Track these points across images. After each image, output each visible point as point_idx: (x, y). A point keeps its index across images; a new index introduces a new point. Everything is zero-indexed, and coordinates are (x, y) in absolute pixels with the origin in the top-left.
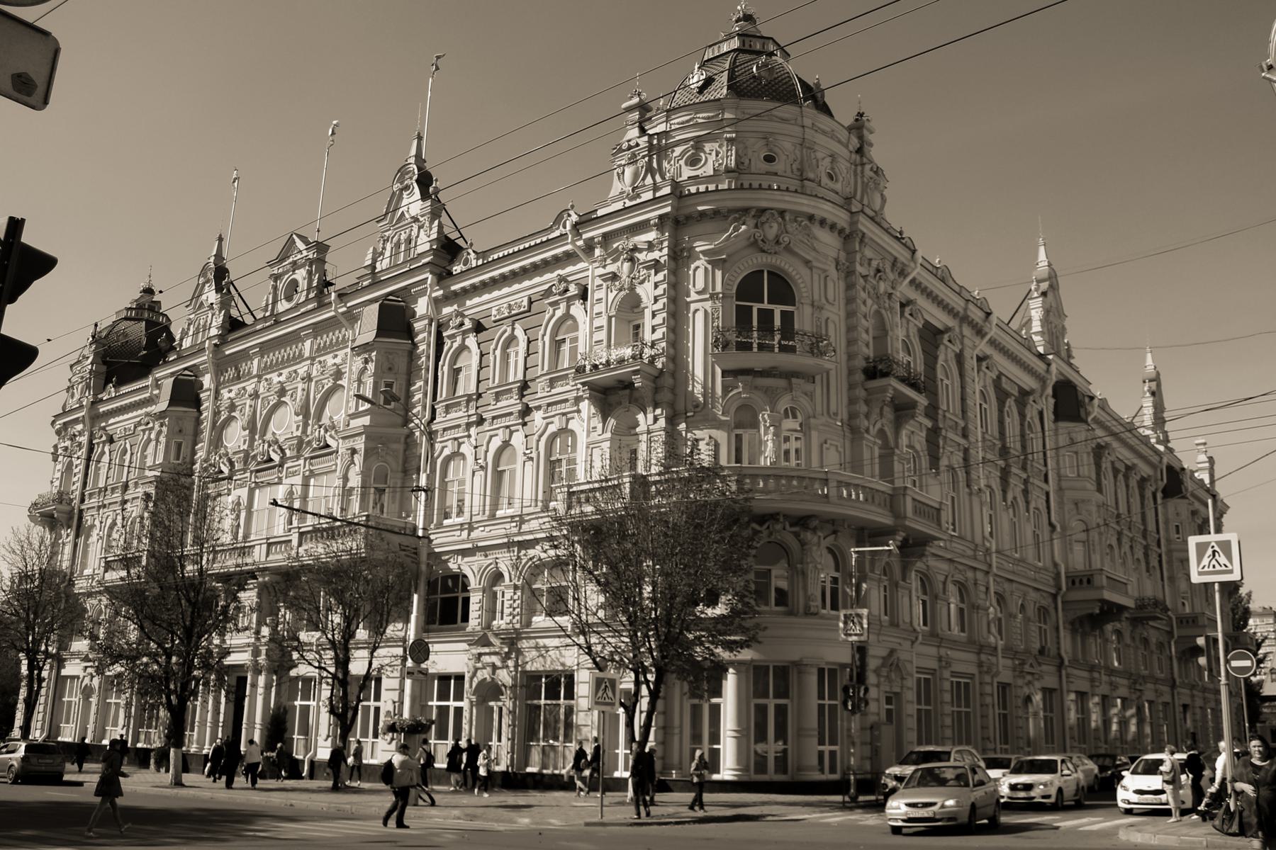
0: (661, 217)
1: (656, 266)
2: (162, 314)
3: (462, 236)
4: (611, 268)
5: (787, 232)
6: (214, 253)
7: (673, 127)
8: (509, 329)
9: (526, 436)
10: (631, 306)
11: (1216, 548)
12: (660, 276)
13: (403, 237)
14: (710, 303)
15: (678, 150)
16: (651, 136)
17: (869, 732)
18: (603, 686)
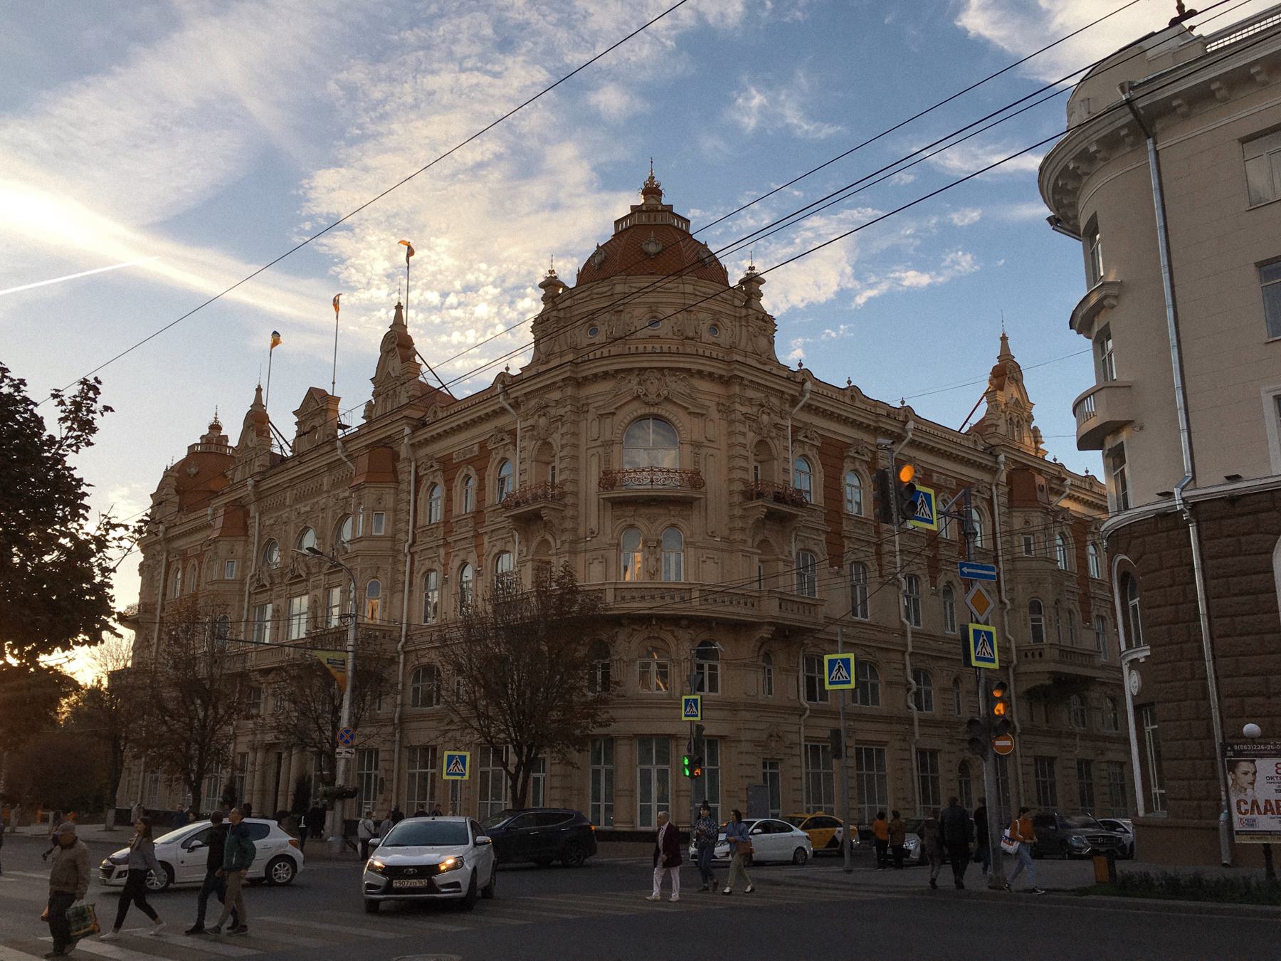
0: (563, 380)
8: (465, 470)
17: (745, 791)
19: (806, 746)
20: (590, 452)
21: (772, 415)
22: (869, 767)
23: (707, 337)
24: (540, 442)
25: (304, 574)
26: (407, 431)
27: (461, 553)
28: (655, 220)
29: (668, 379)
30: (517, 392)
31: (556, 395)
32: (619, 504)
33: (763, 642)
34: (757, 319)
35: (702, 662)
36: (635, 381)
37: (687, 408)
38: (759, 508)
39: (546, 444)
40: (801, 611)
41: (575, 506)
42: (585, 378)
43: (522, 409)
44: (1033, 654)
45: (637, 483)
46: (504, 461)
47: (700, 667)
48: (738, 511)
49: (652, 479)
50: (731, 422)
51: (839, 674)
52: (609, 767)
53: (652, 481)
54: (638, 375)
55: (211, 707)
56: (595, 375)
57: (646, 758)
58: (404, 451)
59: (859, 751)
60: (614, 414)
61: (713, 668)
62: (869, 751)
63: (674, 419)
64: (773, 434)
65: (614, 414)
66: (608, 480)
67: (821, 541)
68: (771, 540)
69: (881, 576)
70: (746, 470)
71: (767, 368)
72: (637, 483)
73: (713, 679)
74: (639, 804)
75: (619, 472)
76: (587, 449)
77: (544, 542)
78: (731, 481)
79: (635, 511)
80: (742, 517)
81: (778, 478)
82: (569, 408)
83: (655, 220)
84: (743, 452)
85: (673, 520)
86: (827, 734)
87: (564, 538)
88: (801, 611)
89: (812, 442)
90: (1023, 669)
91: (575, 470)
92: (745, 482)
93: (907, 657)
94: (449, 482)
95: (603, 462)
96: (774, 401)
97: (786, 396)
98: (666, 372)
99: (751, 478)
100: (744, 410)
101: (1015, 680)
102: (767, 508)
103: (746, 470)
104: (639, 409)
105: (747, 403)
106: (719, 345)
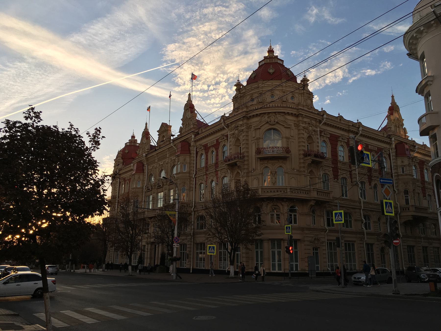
3: (204, 121)
5: (277, 118)
8: (212, 149)
9: (217, 178)
11: (339, 214)
18: (211, 248)
19: (327, 242)
21: (313, 127)
22: (350, 250)
23: (290, 101)
24: (236, 139)
25: (162, 185)
26: (193, 136)
27: (211, 177)
28: (272, 61)
29: (278, 116)
30: (228, 122)
31: (241, 123)
32: (262, 159)
33: (312, 206)
34: (307, 94)
35: (291, 213)
36: (266, 117)
37: (284, 126)
38: (309, 160)
39: (238, 140)
40: (324, 195)
41: (248, 160)
42: (250, 117)
43: (230, 128)
44: (406, 209)
45: (268, 152)
46: (224, 145)
47: (291, 215)
48: (302, 161)
49: (273, 150)
50: (299, 130)
51: (338, 218)
52: (261, 250)
53: (273, 151)
54: (268, 115)
55: (134, 230)
56: (253, 115)
57: (273, 247)
58: (192, 144)
59: (345, 244)
60: (260, 128)
61: (295, 216)
62: (349, 244)
63: (280, 130)
64: (313, 134)
65: (260, 128)
66: (259, 151)
67: (331, 170)
68: (314, 171)
69: (352, 182)
70: (305, 146)
71: (311, 111)
72: (268, 152)
73: (295, 219)
74: (271, 263)
75: (262, 148)
76: (251, 141)
77: (238, 173)
78: (299, 150)
79: (268, 162)
80: (303, 163)
81: (315, 149)
82: (245, 127)
83: (272, 61)
84: (303, 140)
85: (281, 164)
86: (335, 238)
87: (244, 172)
88: (324, 195)
89: (326, 136)
90: (403, 214)
91: (247, 148)
92: (304, 151)
93: (362, 211)
94: (207, 153)
95: (256, 146)
96: (313, 122)
97: (318, 120)
98: (277, 113)
99: (306, 149)
100: (303, 125)
101: (400, 218)
102: (312, 159)
103: (305, 146)
105: (304, 123)
106: (294, 103)
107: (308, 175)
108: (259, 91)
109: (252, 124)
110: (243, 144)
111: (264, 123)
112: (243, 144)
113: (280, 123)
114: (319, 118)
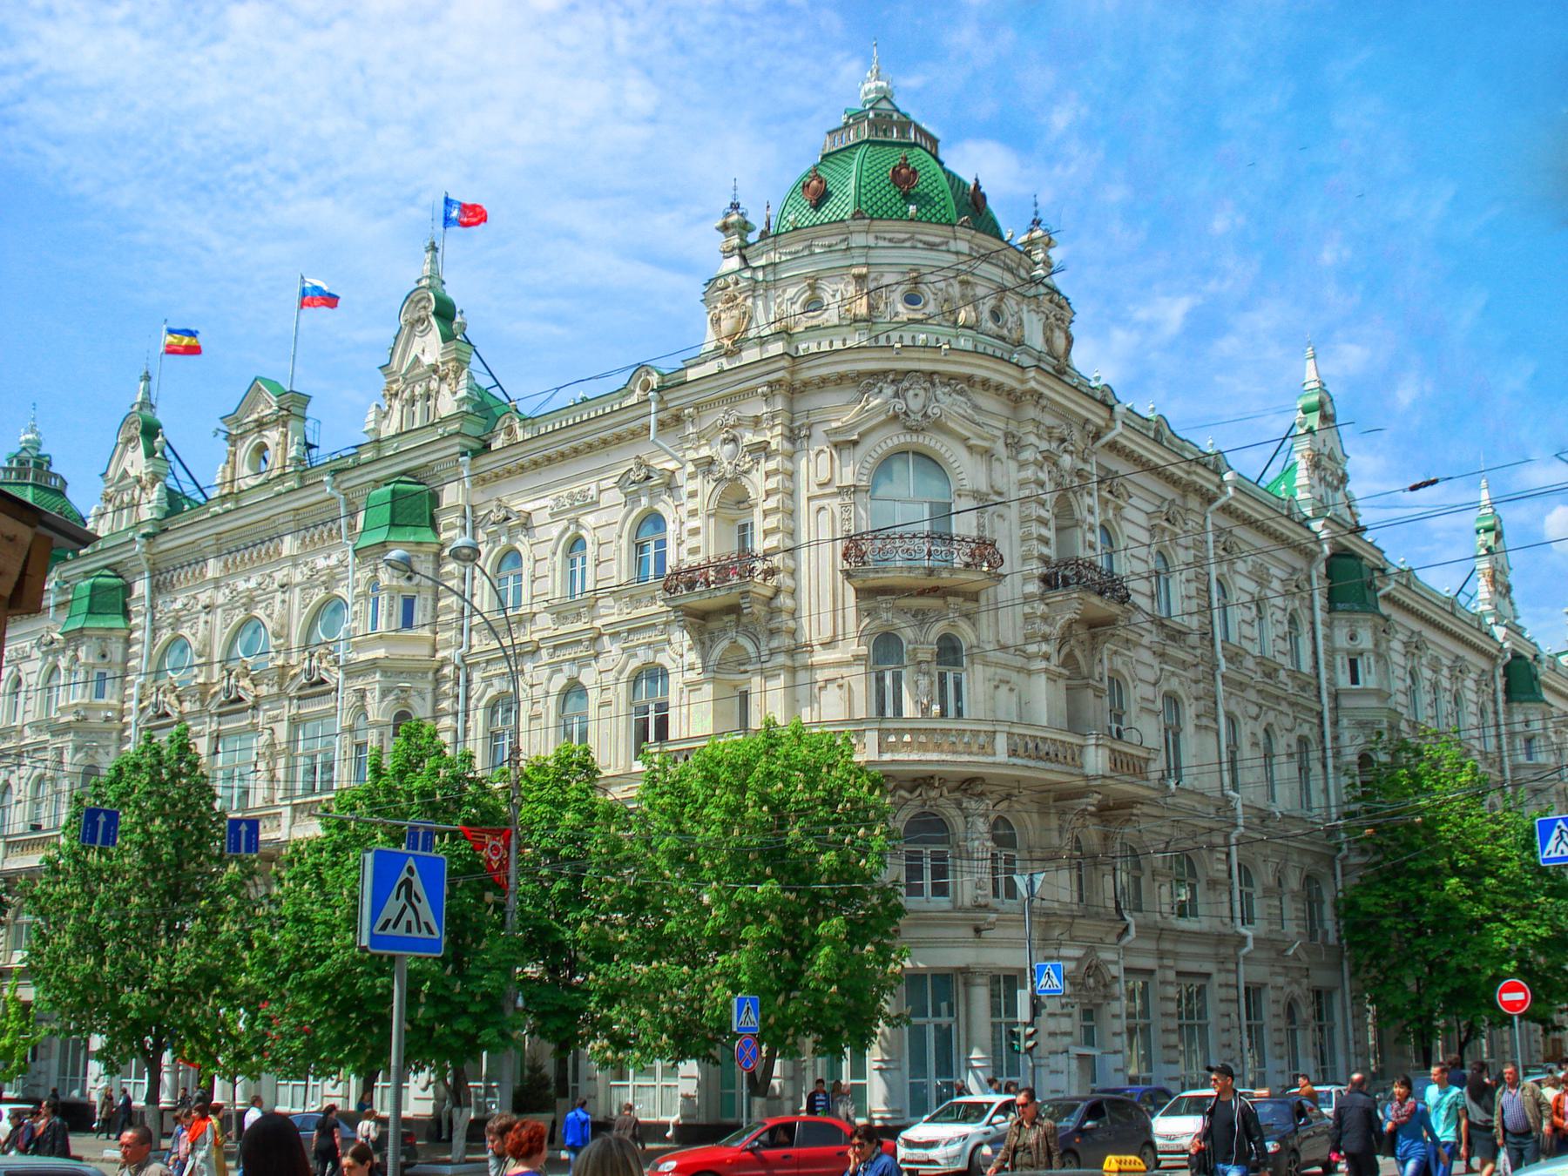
0: (770, 384)
1: (763, 450)
2: (56, 476)
3: (498, 384)
4: (705, 452)
5: (937, 401)
6: (139, 400)
7: (784, 258)
10: (734, 499)
12: (772, 465)
13: (418, 390)
14: (838, 500)
15: (791, 292)
16: (755, 269)
20: (815, 504)
29: (941, 391)
36: (889, 391)
38: (1071, 605)
42: (806, 384)
54: (893, 381)
60: (855, 443)
65: (855, 443)
80: (1045, 618)
82: (778, 430)
87: (774, 644)
92: (1045, 560)
104: (897, 438)
107: (1060, 675)
108: (851, 266)
109: (813, 419)
110: (766, 514)
111: (874, 422)
112: (766, 514)
113: (950, 424)
114: (1097, 416)
